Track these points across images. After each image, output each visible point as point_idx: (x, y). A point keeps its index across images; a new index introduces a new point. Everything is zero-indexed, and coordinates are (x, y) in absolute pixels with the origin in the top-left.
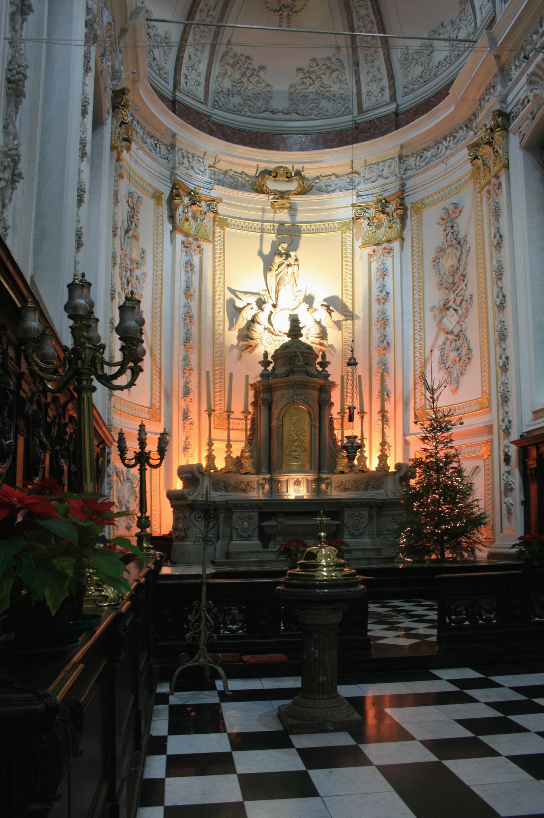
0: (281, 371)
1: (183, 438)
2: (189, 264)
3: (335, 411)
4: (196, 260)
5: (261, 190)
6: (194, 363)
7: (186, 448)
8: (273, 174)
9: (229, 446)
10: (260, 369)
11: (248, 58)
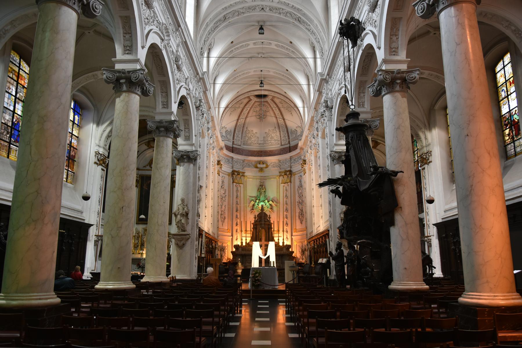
0: (258, 220)
1: (236, 237)
2: (237, 190)
3: (273, 230)
4: (239, 189)
5: (257, 167)
6: (239, 217)
7: (237, 240)
8: (259, 162)
9: (246, 239)
10: (254, 219)
11: (252, 130)
